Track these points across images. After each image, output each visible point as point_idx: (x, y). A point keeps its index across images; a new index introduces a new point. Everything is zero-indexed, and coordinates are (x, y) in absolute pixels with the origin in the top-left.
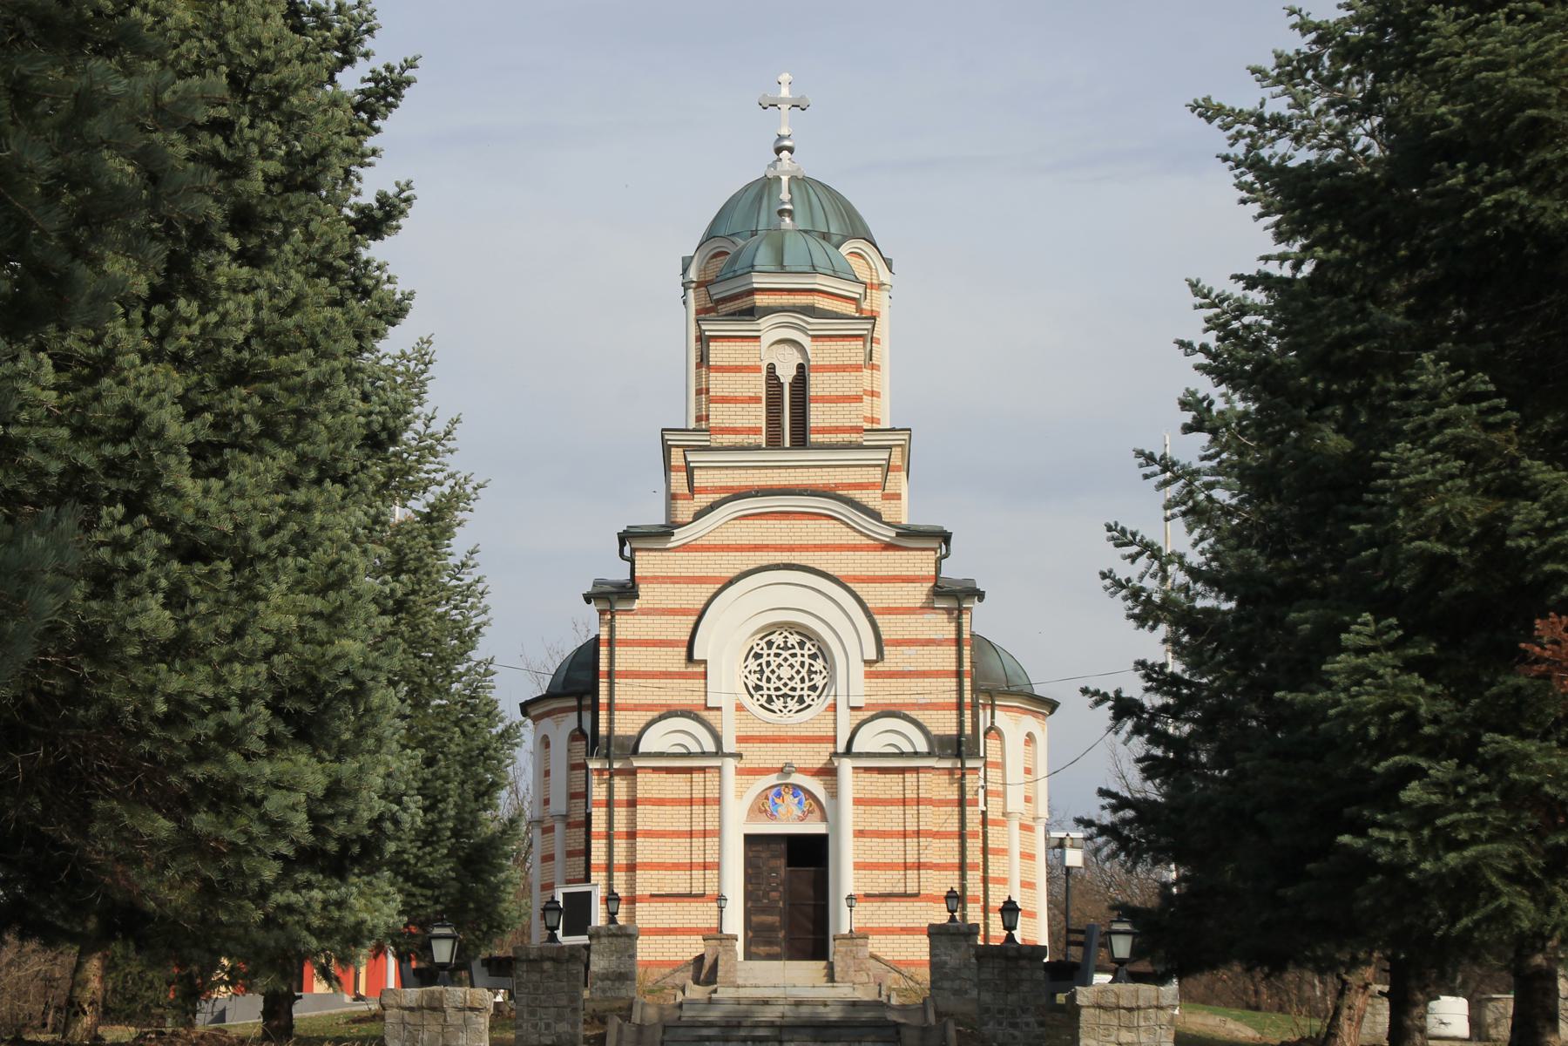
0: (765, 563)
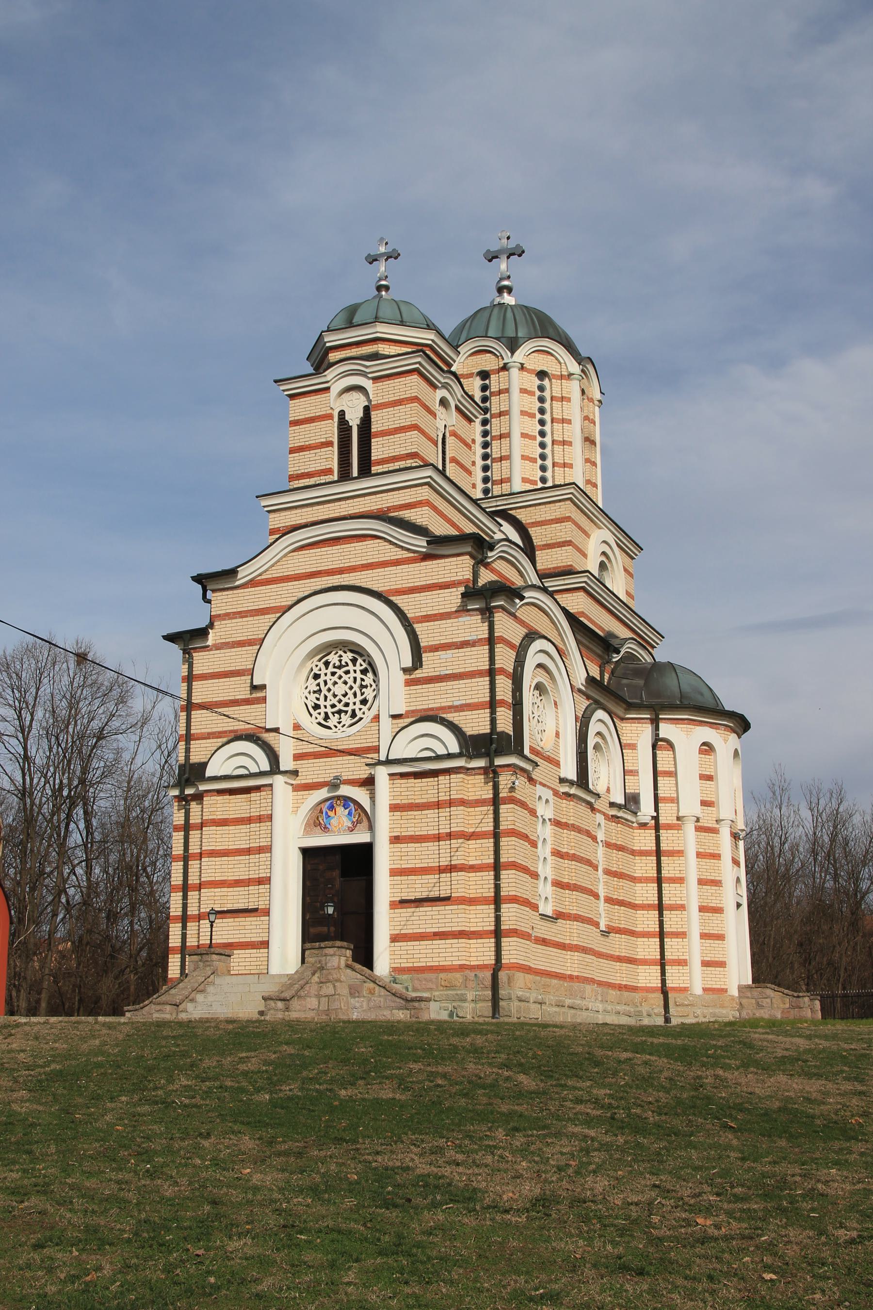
0: (319, 588)
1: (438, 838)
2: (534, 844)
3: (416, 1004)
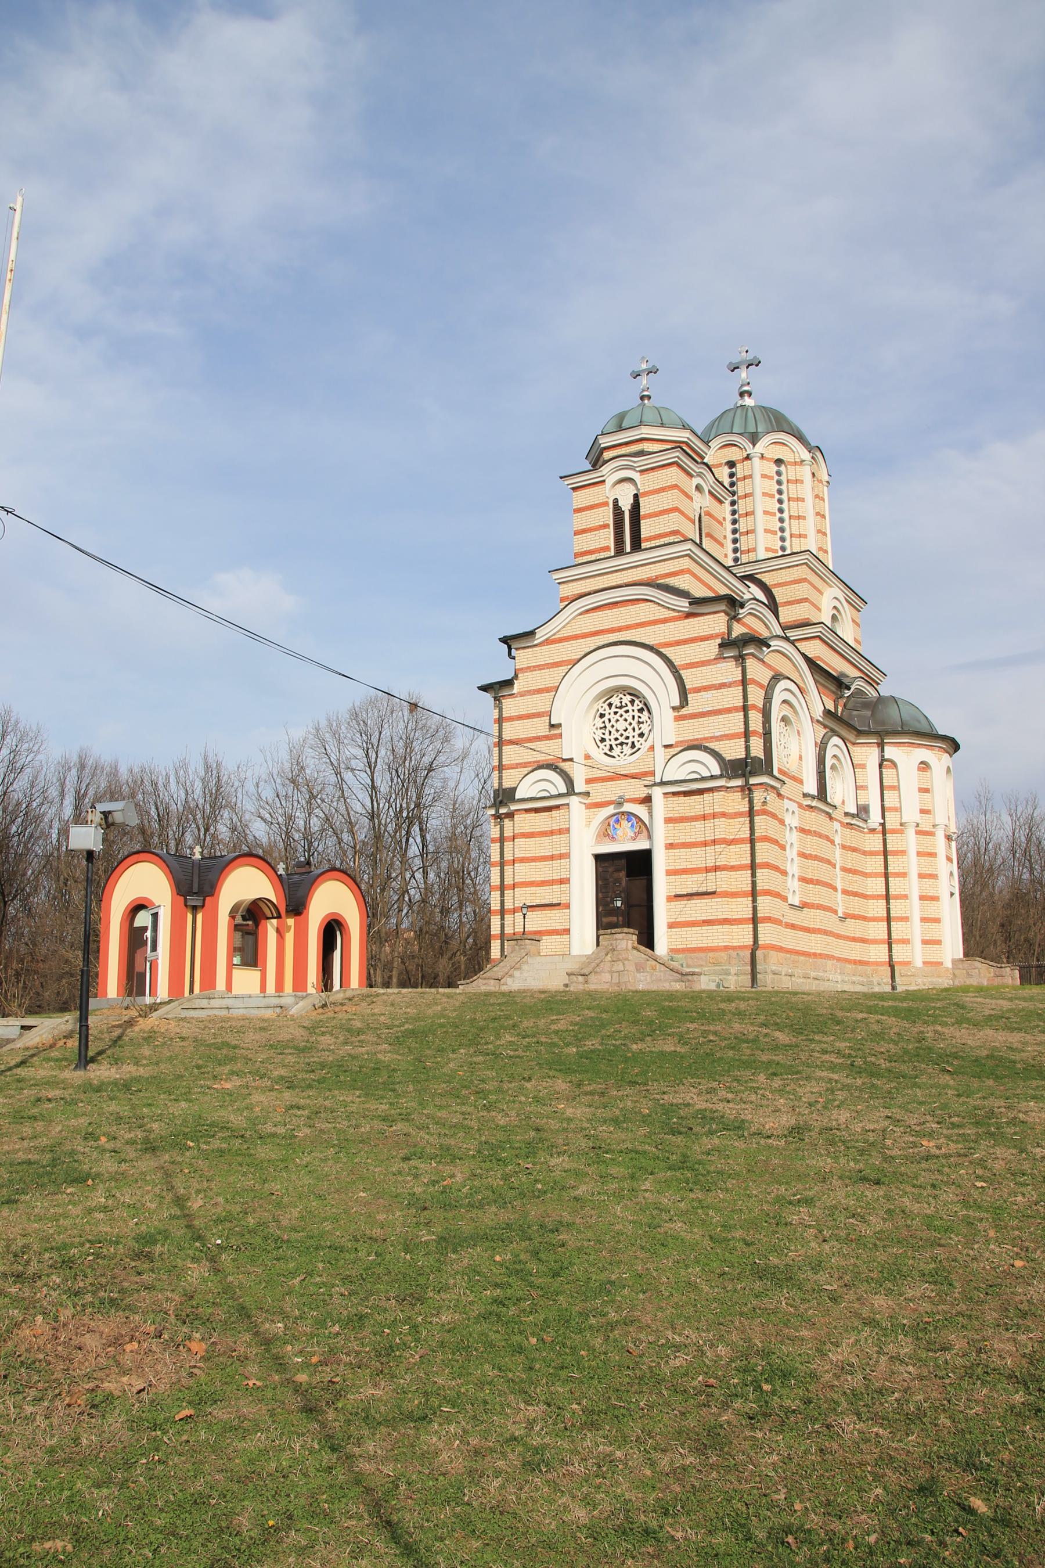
0: (602, 643)
1: (705, 844)
2: (783, 848)
3: (690, 977)
